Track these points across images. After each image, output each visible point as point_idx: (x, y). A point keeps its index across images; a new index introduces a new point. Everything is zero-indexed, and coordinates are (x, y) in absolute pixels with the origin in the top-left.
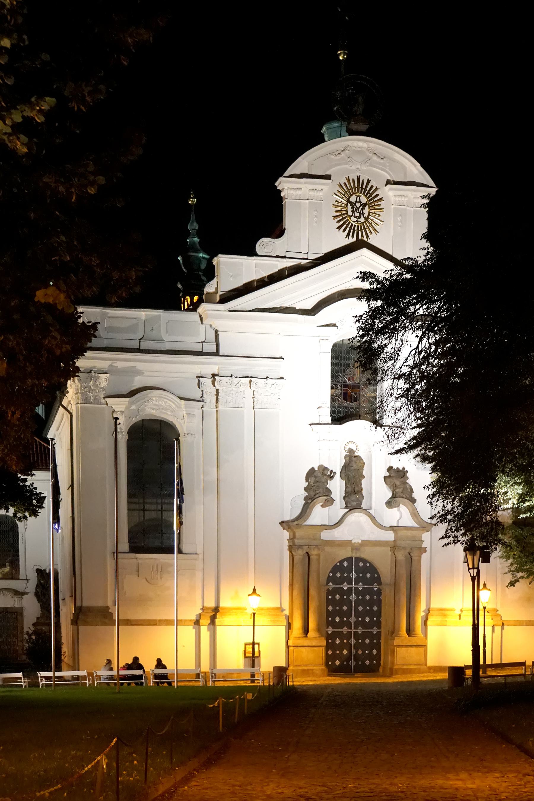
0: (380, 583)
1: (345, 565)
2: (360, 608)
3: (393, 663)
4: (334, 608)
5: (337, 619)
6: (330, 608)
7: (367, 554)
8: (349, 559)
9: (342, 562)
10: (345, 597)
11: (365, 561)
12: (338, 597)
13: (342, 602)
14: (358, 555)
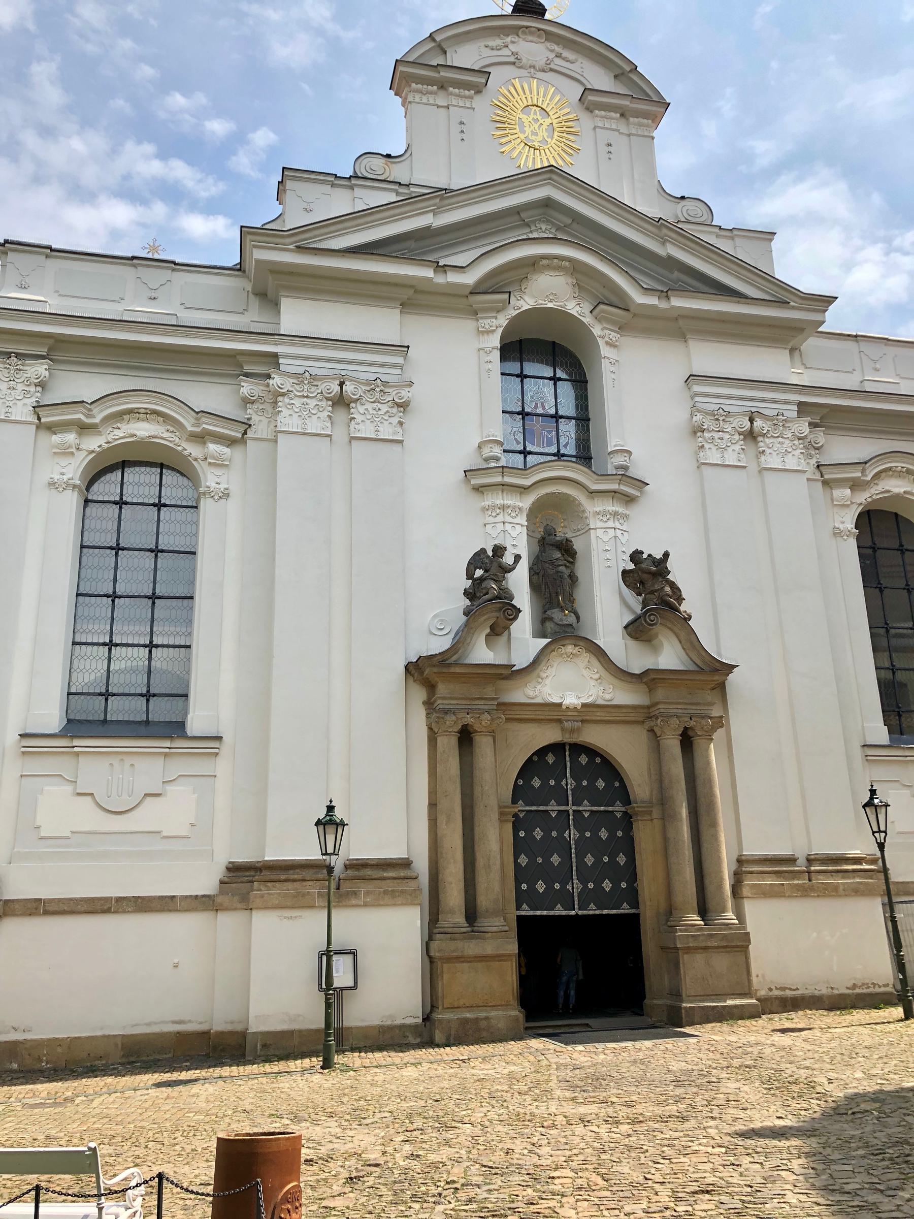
0: (627, 801)
1: (551, 762)
3: (677, 994)
5: (541, 887)
6: (523, 860)
7: (594, 736)
8: (556, 748)
9: (542, 752)
10: (554, 834)
11: (591, 752)
12: (538, 834)
13: (547, 846)
14: (574, 739)
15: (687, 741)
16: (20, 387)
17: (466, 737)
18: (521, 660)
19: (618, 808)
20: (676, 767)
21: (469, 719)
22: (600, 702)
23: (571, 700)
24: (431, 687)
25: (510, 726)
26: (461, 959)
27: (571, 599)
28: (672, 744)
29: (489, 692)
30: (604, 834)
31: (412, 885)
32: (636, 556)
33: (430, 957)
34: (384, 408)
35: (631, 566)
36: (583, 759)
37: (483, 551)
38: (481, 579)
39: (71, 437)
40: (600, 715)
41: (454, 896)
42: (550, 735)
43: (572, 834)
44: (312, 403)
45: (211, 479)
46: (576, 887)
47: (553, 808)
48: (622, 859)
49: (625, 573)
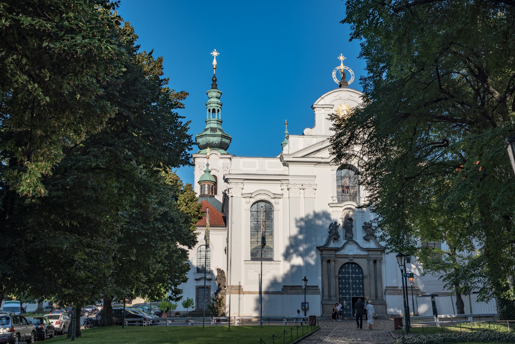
2: (354, 286)
4: (342, 286)
6: (340, 286)
7: (356, 261)
8: (348, 263)
11: (355, 264)
12: (344, 281)
15: (375, 262)
16: (238, 189)
17: (329, 261)
18: (340, 246)
19: (361, 275)
20: (372, 268)
21: (329, 259)
22: (357, 254)
23: (351, 253)
24: (321, 251)
25: (338, 259)
26: (328, 304)
27: (352, 231)
28: (372, 263)
29: (333, 252)
30: (357, 281)
31: (318, 291)
32: (365, 223)
33: (322, 304)
34: (311, 190)
35: (364, 225)
36: (354, 265)
37: (332, 223)
38: (332, 229)
39: (248, 199)
40: (357, 257)
41: (326, 293)
42: (347, 260)
43: (351, 281)
44: (296, 190)
45: (276, 207)
46: (351, 291)
47: (347, 275)
48: (361, 286)
49: (363, 226)
